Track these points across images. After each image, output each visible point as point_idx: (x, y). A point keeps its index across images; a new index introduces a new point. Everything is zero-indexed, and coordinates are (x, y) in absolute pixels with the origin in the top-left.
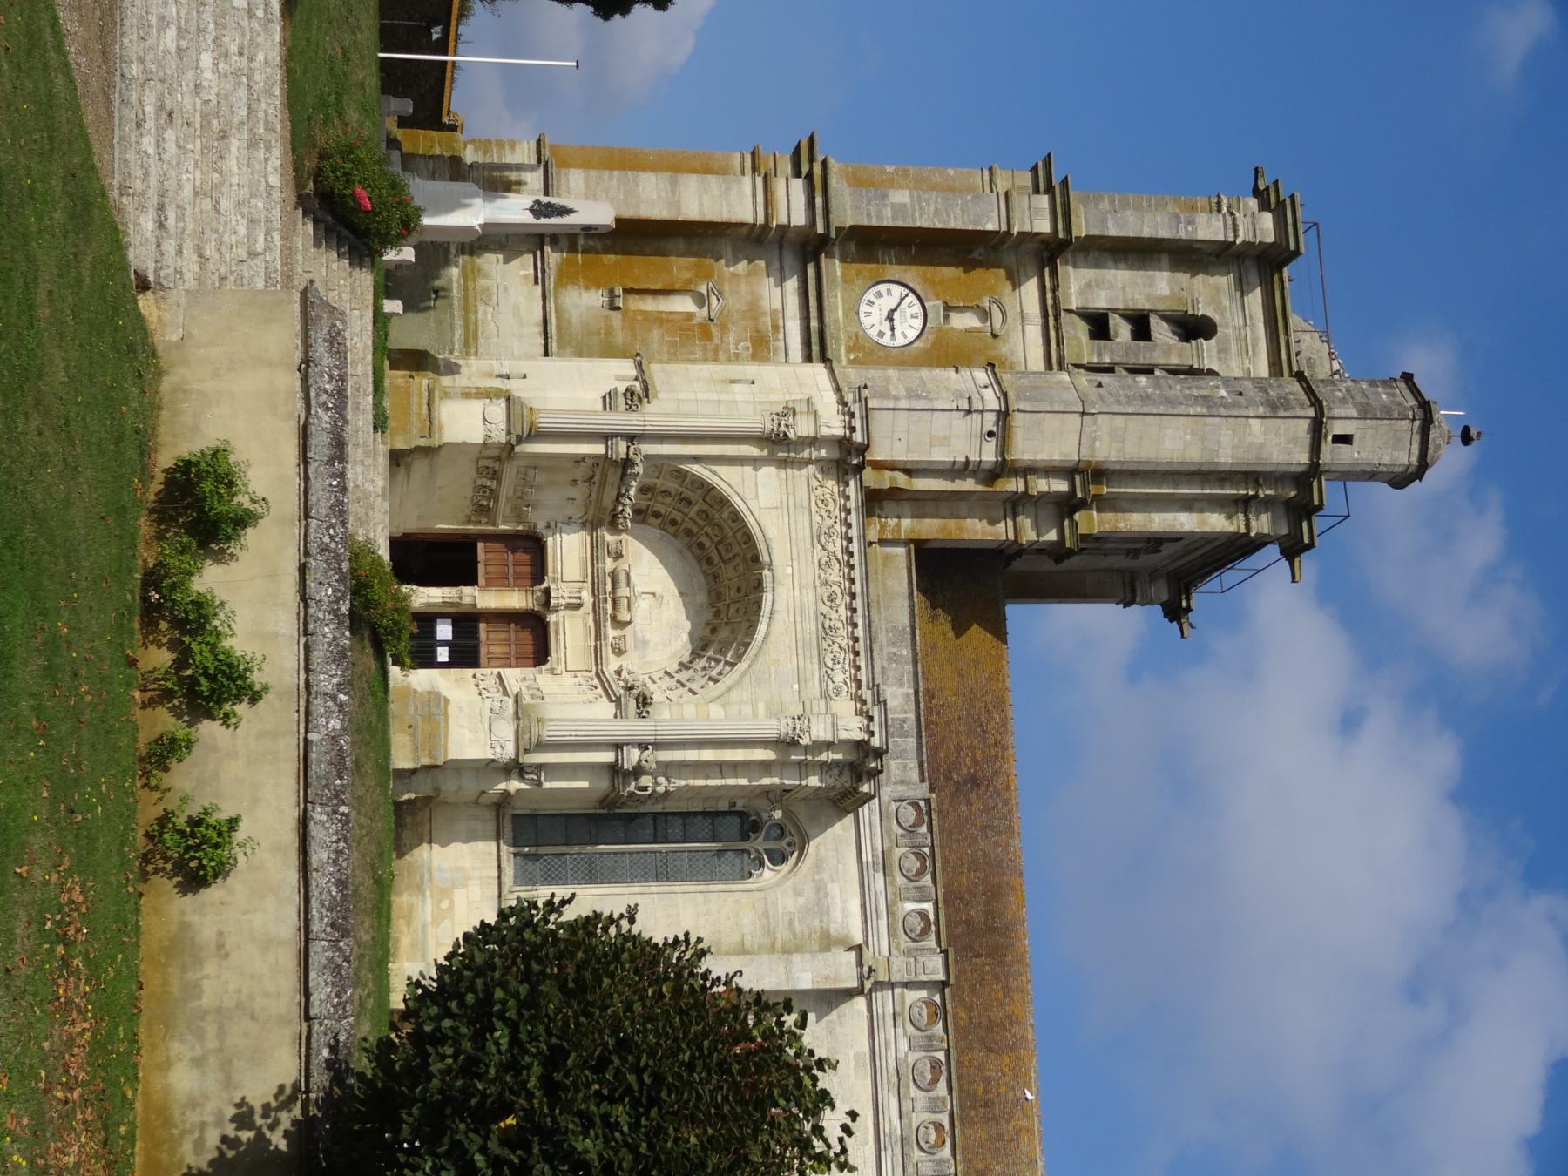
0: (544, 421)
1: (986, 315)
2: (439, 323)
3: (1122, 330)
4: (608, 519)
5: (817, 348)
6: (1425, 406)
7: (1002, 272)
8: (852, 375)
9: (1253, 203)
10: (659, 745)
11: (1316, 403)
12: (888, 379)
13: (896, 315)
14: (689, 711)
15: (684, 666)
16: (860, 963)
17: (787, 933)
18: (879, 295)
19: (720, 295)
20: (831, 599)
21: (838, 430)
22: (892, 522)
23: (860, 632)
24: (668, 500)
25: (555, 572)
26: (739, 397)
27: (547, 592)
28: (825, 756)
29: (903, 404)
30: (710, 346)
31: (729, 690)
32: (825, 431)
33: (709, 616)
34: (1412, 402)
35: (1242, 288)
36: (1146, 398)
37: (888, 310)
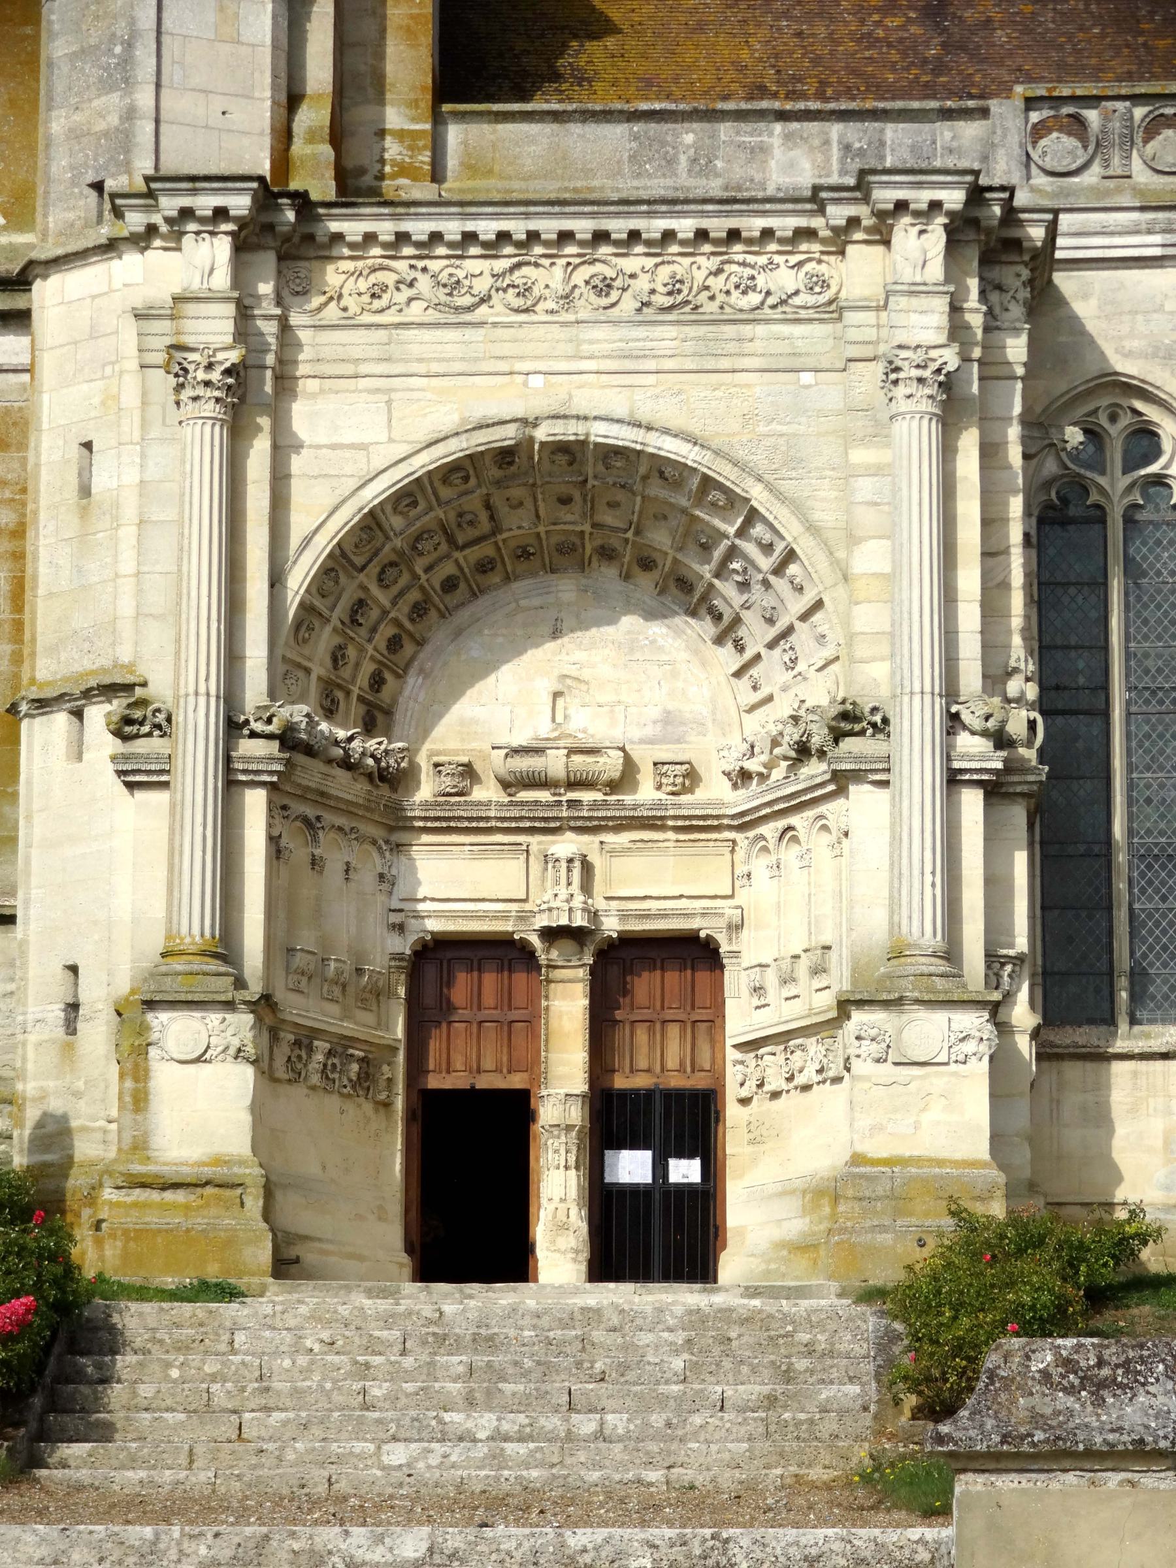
0: (196, 924)
4: (384, 790)
8: (65, 215)
10: (951, 692)
12: (75, 134)
14: (869, 618)
15: (728, 632)
20: (604, 287)
21: (222, 248)
22: (393, 149)
23: (685, 226)
24: (351, 652)
25: (504, 916)
26: (131, 476)
27: (551, 934)
28: (976, 320)
29: (145, 98)
31: (812, 529)
32: (222, 280)
33: (609, 573)
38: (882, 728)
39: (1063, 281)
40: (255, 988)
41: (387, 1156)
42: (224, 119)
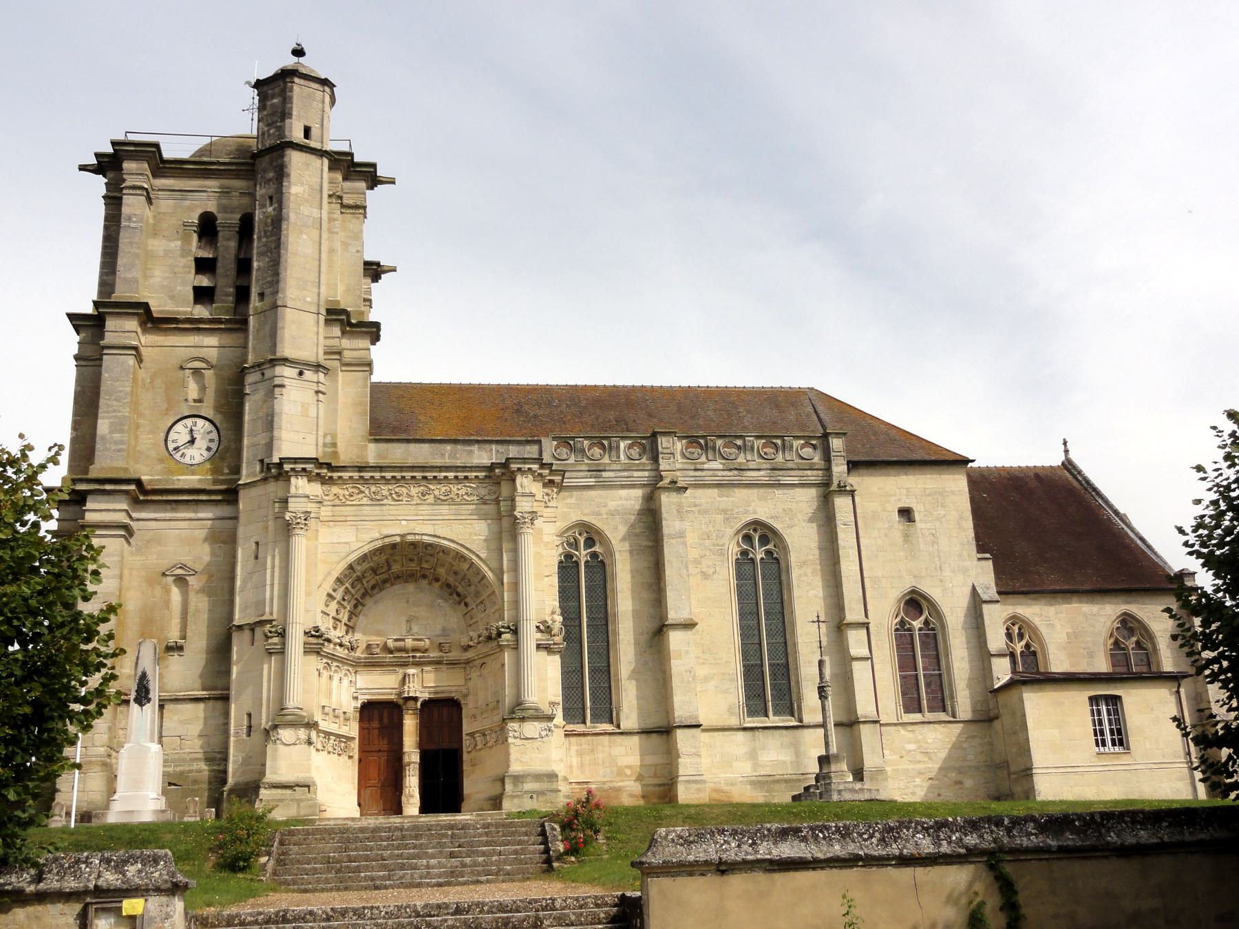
33: (424, 582)
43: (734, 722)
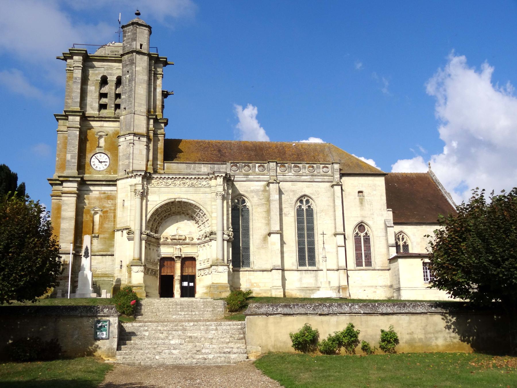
0: (137, 256)
1: (101, 137)
2: (102, 284)
3: (104, 101)
5: (112, 183)
6: (133, 24)
7: (88, 131)
8: (121, 174)
9: (68, 61)
10: (223, 230)
11: (132, 52)
12: (123, 164)
13: (100, 161)
14: (214, 222)
15: (197, 222)
16: (273, 183)
17: (263, 200)
18: (94, 165)
19: (95, 208)
20: (184, 184)
21: (141, 178)
22: (159, 166)
23: (193, 177)
27: (176, 257)
28: (226, 188)
29: (131, 161)
30: (109, 211)
31: (207, 211)
32: (141, 182)
33: (183, 215)
34: (131, 27)
35: (93, 67)
36: (129, 97)
37: (99, 163)
38: (215, 234)
39: (234, 183)
40: (143, 264)
41: (156, 283)
42: (140, 163)
43: (295, 268)
